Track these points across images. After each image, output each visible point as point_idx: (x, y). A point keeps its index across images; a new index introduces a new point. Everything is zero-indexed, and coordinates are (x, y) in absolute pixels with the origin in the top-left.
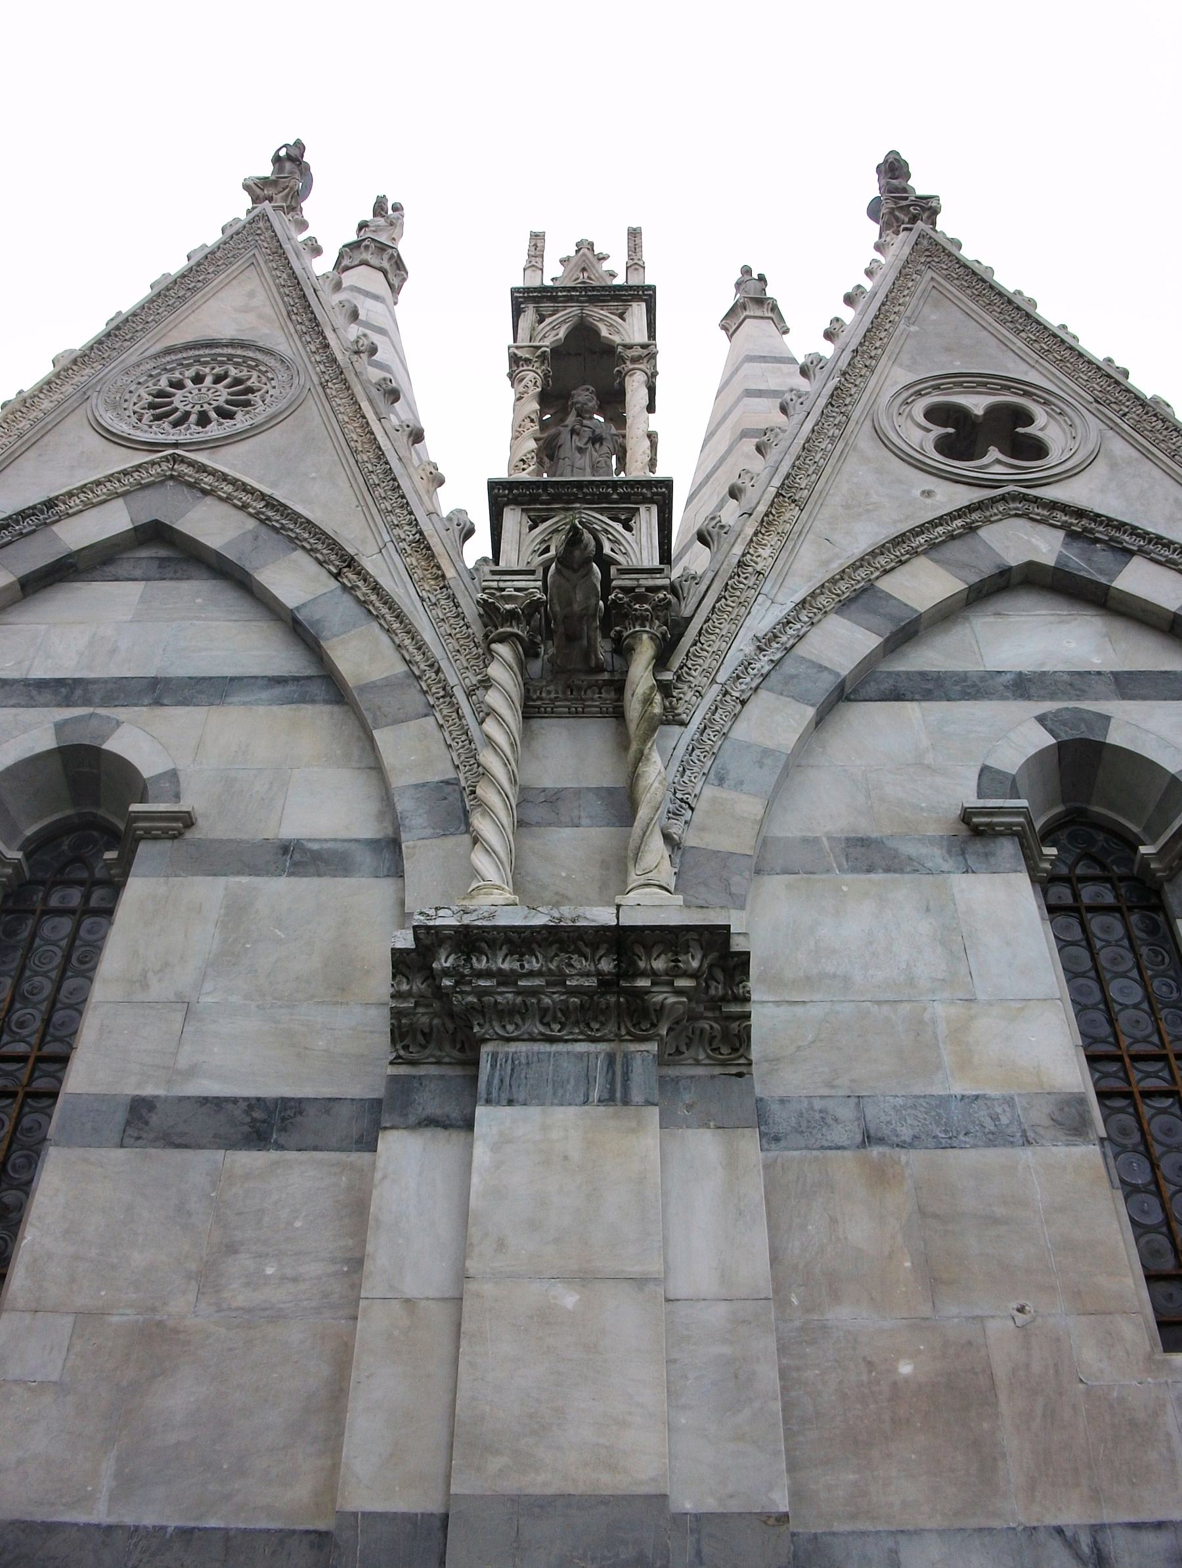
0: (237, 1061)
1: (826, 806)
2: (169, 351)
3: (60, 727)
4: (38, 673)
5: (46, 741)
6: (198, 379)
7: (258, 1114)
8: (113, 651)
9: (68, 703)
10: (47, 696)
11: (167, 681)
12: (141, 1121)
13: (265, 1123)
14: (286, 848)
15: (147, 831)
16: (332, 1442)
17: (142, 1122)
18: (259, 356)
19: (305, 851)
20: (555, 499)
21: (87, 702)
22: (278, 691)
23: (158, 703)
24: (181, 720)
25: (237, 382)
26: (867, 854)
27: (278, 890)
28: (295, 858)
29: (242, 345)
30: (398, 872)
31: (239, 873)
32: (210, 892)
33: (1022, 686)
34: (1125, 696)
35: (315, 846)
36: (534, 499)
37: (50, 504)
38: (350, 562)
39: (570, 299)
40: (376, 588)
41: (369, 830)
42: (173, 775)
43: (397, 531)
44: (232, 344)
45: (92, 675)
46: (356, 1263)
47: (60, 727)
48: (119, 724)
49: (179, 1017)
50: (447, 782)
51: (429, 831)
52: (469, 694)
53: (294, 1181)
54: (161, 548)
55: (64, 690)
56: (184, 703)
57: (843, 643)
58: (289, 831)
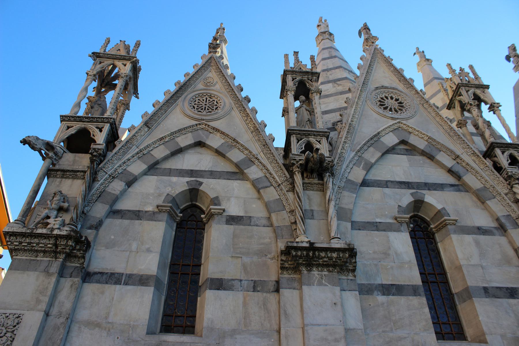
2: (377, 88)
3: (412, 194)
4: (398, 179)
5: (412, 199)
6: (387, 98)
7: (509, 291)
8: (411, 174)
9: (409, 188)
10: (403, 186)
11: (428, 183)
14: (479, 228)
15: (449, 223)
18: (400, 93)
19: (483, 229)
20: (506, 147)
21: (414, 188)
22: (452, 188)
23: (429, 190)
27: (482, 238)
28: (481, 231)
29: (394, 89)
31: (472, 234)
32: (469, 238)
35: (484, 228)
36: (502, 147)
37: (379, 133)
38: (458, 157)
39: (472, 87)
40: (467, 164)
43: (465, 150)
44: (391, 88)
45: (410, 181)
47: (412, 194)
48: (424, 195)
49: (480, 268)
50: (508, 215)
51: (512, 227)
52: (506, 194)
55: (407, 185)
56: (435, 190)
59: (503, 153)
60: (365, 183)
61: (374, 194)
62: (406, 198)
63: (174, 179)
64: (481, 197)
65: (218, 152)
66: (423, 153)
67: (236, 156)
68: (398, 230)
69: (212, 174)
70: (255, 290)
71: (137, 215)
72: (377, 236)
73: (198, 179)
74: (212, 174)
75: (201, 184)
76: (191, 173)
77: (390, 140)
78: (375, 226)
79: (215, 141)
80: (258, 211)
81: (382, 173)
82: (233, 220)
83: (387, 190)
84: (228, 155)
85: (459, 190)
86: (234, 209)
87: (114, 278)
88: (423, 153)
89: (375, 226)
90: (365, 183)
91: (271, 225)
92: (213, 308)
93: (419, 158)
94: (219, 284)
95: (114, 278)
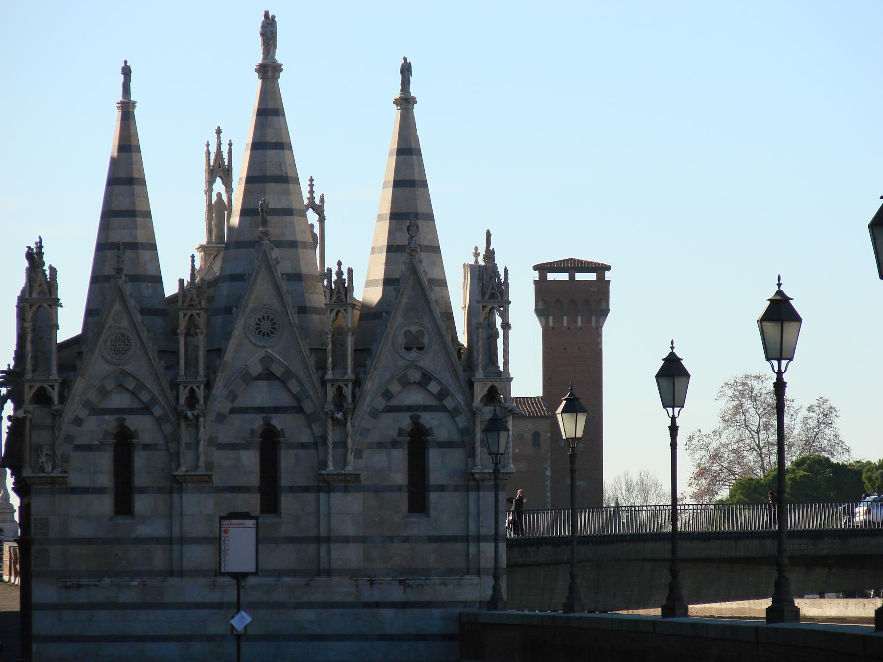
0: (302, 482)
1: (374, 437)
3: (263, 418)
4: (256, 405)
12: (292, 489)
13: (306, 489)
16: (319, 527)
17: (292, 489)
24: (281, 416)
25: (272, 320)
26: (380, 445)
27: (302, 452)
28: (303, 446)
30: (317, 449)
32: (292, 452)
33: (409, 408)
34: (424, 411)
41: (312, 441)
42: (282, 429)
46: (319, 508)
53: (310, 497)
54: (269, 376)
55: (260, 410)
57: (381, 403)
58: (302, 441)
59: (332, 385)
60: (233, 411)
61: (236, 419)
62: (257, 422)
63: (107, 417)
64: (310, 419)
65: (133, 394)
66: (278, 379)
67: (145, 397)
68: (246, 449)
69: (131, 411)
70: (160, 493)
71: (89, 448)
72: (232, 454)
73: (124, 416)
74: (131, 411)
75: (124, 420)
76: (118, 411)
77: (256, 369)
78: (233, 447)
79: (131, 385)
80: (160, 441)
81: (243, 401)
82: (146, 447)
83: (246, 416)
84: (140, 396)
85: (297, 412)
86: (146, 437)
87: (84, 491)
88: (278, 379)
89: (233, 447)
90: (233, 411)
91: (168, 449)
92: (141, 504)
93: (276, 382)
94: (142, 491)
95: (84, 491)
